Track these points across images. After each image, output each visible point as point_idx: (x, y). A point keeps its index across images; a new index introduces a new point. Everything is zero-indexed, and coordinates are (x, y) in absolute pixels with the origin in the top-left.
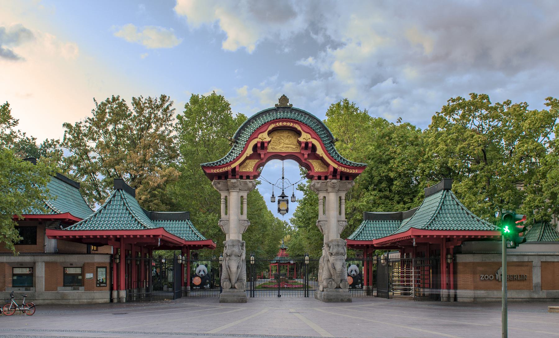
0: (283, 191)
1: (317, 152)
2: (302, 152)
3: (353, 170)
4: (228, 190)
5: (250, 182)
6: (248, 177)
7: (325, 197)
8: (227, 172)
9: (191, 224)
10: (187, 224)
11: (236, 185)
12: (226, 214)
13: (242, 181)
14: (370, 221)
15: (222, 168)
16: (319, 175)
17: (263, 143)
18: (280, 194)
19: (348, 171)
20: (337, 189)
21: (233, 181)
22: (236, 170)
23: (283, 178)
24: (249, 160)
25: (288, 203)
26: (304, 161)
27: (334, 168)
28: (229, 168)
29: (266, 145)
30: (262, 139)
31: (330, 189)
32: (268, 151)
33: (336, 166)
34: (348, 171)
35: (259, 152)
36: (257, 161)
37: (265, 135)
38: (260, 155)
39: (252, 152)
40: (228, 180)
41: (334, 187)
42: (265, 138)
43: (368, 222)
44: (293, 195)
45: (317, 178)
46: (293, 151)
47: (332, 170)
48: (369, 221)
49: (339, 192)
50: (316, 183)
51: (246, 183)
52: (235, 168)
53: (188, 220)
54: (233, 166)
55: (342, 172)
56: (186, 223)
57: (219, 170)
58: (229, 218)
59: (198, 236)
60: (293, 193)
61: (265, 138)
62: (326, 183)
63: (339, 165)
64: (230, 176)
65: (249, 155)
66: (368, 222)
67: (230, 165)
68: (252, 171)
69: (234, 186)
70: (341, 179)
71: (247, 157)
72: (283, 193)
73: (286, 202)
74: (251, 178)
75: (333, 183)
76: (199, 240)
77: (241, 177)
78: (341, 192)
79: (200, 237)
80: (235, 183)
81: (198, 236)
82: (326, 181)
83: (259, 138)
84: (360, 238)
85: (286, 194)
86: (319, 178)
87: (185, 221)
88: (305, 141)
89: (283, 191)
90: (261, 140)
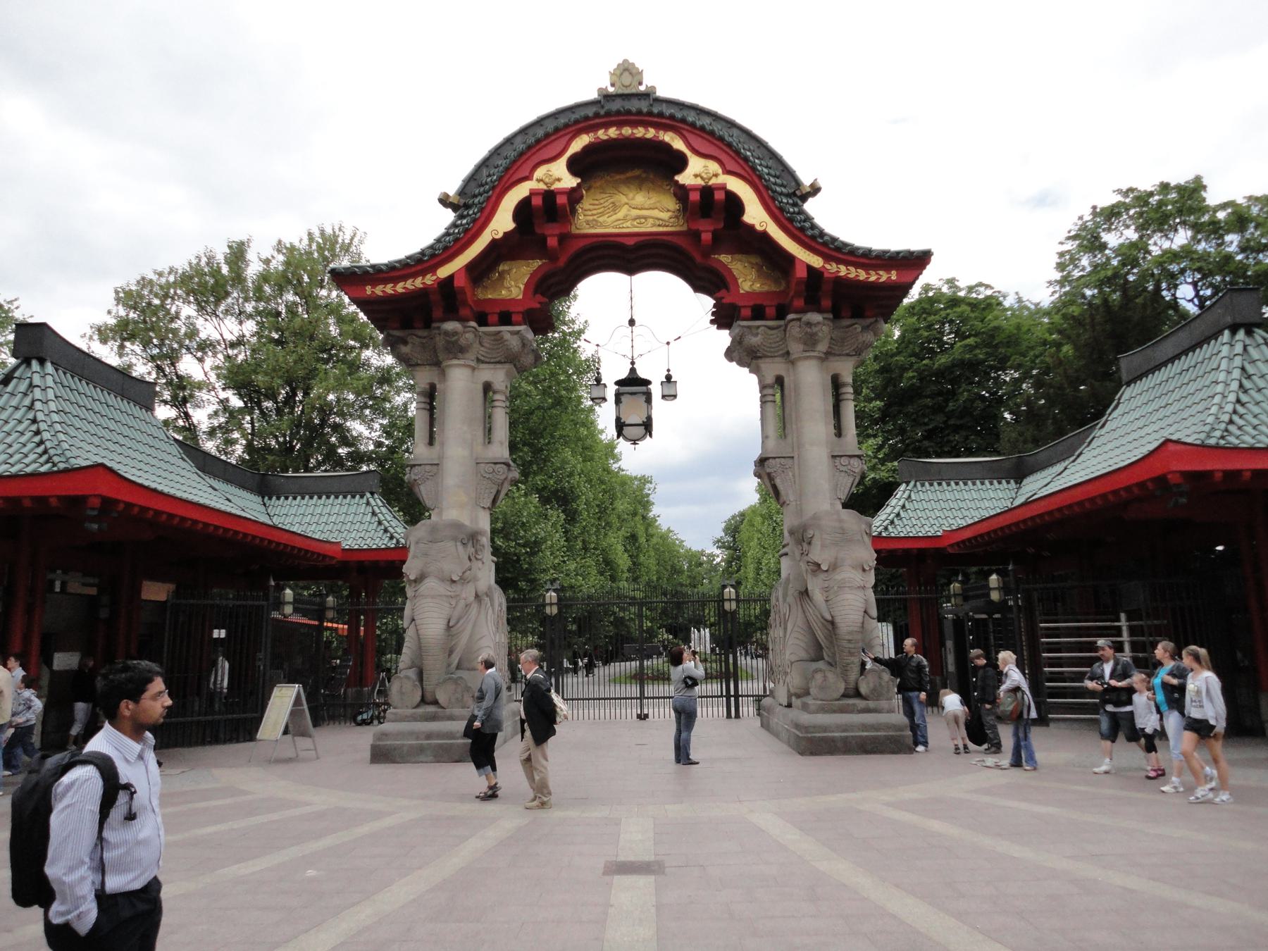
0: (633, 363)
1: (747, 218)
2: (694, 227)
3: (881, 273)
4: (437, 364)
5: (513, 333)
6: (505, 319)
7: (780, 381)
8: (424, 292)
9: (380, 504)
10: (368, 503)
11: (462, 342)
12: (431, 442)
13: (484, 333)
14: (923, 485)
15: (404, 278)
16: (758, 302)
17: (549, 196)
18: (623, 374)
19: (862, 275)
20: (822, 347)
21: (450, 326)
22: (455, 285)
23: (632, 322)
24: (509, 262)
25: (649, 400)
26: (698, 258)
27: (810, 268)
28: (429, 280)
29: (562, 200)
30: (547, 180)
31: (796, 348)
32: (574, 231)
33: (816, 261)
34: (861, 278)
35: (538, 231)
36: (536, 264)
38: (543, 240)
39: (510, 225)
40: (435, 325)
41: (810, 341)
42: (559, 180)
43: (915, 486)
44: (669, 378)
45: (746, 312)
46: (661, 229)
47: (801, 273)
48: (918, 483)
49: (831, 358)
50: (745, 329)
51: (497, 337)
52: (451, 278)
53: (372, 494)
54: (444, 272)
55: (839, 281)
56: (364, 500)
57: (394, 286)
58: (441, 457)
59: (392, 538)
60: (668, 370)
61: (559, 180)
62: (782, 328)
63: (827, 258)
64: (437, 313)
65: (500, 235)
66: (915, 486)
67: (433, 269)
68: (521, 297)
69: (455, 349)
70: (837, 314)
71: (494, 243)
72: (633, 370)
73: (644, 398)
74: (514, 318)
75: (809, 324)
76: (393, 546)
77: (482, 320)
78: (837, 358)
79: (398, 542)
80: (455, 333)
81: (392, 538)
82: (782, 323)
83: (539, 181)
84: (893, 532)
85: (642, 373)
86: (758, 313)
87: (362, 497)
88: (700, 182)
89: (633, 363)
90: (542, 186)
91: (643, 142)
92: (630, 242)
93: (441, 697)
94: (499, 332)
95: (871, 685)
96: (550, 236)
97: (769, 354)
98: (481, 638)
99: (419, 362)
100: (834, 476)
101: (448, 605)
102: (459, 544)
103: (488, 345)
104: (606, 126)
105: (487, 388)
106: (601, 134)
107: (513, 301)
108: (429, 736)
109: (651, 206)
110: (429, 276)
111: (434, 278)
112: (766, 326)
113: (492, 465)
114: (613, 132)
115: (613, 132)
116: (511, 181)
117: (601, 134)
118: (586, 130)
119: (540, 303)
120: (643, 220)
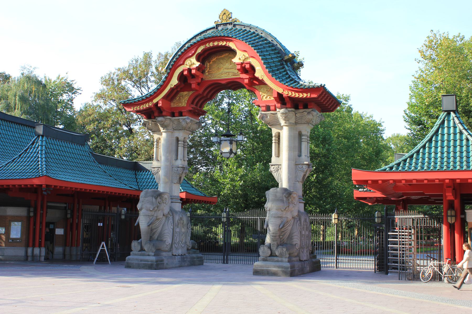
1: (257, 75)
3: (304, 94)
6: (181, 114)
17: (189, 70)
27: (278, 93)
28: (151, 104)
35: (189, 82)
37: (193, 60)
38: (191, 84)
45: (264, 108)
52: (157, 103)
54: (155, 101)
61: (194, 64)
64: (156, 114)
67: (152, 100)
68: (185, 106)
77: (173, 115)
91: (222, 46)
92: (223, 82)
93: (146, 248)
94: (179, 119)
95: (279, 252)
96: (193, 83)
97: (274, 124)
98: (164, 230)
99: (155, 130)
100: (296, 172)
101: (149, 219)
102: (153, 198)
103: (176, 124)
104: (209, 42)
105: (177, 140)
106: (207, 45)
107: (183, 107)
108: (141, 261)
109: (231, 68)
110: (150, 103)
111: (152, 103)
112: (271, 113)
113: (177, 168)
114: (211, 44)
115: (211, 44)
116: (177, 66)
117: (207, 45)
118: (202, 44)
119: (192, 108)
120: (228, 74)
